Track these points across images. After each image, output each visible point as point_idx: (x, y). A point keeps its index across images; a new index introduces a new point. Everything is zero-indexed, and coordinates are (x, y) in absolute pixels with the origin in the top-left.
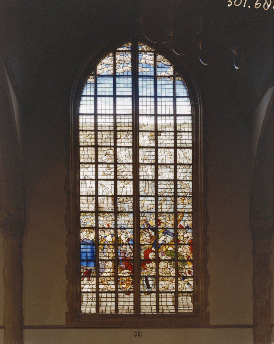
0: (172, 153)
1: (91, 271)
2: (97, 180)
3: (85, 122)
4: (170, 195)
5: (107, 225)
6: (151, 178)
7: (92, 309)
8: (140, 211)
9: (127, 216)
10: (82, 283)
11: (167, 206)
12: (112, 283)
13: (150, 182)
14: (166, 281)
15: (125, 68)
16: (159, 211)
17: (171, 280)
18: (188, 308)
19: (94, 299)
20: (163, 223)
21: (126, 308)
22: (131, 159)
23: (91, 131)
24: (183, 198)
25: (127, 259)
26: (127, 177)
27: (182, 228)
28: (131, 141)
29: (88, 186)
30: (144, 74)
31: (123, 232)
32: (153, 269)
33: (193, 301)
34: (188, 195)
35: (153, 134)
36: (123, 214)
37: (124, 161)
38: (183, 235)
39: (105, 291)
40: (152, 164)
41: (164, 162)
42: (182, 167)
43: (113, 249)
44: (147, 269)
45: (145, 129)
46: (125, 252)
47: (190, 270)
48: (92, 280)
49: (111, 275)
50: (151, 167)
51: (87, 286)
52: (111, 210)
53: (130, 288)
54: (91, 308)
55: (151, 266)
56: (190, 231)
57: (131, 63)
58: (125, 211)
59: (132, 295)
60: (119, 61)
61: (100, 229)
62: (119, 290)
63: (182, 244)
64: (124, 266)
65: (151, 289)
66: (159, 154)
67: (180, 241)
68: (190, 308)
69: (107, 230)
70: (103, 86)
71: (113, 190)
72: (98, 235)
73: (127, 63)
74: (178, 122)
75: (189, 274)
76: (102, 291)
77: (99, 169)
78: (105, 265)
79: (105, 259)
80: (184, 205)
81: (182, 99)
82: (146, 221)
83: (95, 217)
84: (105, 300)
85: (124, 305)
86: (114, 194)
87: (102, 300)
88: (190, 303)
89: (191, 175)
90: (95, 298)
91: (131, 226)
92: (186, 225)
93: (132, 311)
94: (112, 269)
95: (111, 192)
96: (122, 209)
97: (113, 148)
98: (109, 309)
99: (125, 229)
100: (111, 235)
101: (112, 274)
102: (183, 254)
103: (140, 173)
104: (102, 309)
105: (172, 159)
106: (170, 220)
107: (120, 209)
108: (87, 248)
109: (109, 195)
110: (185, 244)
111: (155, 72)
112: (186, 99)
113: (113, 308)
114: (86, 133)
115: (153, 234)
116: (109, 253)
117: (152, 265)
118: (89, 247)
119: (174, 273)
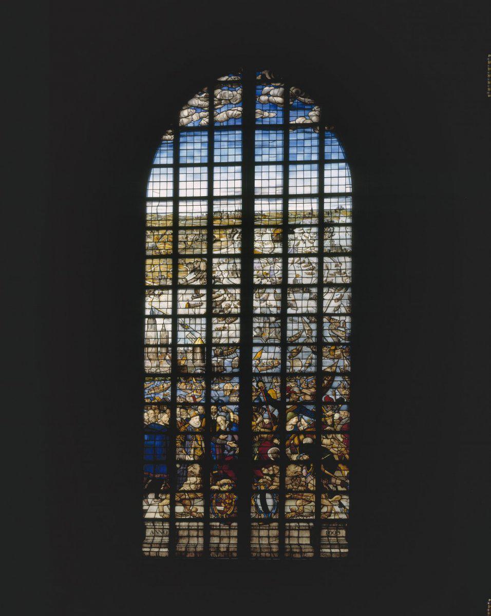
0: (314, 265)
1: (160, 481)
2: (175, 317)
3: (156, 212)
4: (308, 341)
5: (191, 398)
6: (274, 311)
7: (161, 550)
10: (144, 503)
11: (304, 361)
12: (198, 504)
13: (273, 319)
14: (298, 499)
15: (230, 112)
16: (288, 371)
17: (309, 498)
18: (337, 550)
19: (165, 532)
20: (295, 393)
21: (223, 548)
22: (238, 277)
23: (167, 228)
24: (333, 348)
25: (226, 459)
26: (229, 309)
27: (330, 402)
28: (238, 244)
30: (266, 121)
33: (347, 537)
34: (343, 341)
35: (279, 231)
37: (225, 282)
38: (333, 416)
39: (187, 517)
40: (274, 286)
41: (299, 281)
42: (333, 291)
45: (265, 222)
46: (223, 446)
47: (343, 479)
49: (198, 489)
50: (275, 291)
51: (154, 508)
52: (199, 371)
53: (233, 512)
54: (160, 548)
55: (271, 473)
56: (345, 407)
57: (241, 104)
58: (225, 372)
59: (235, 524)
60: (220, 100)
62: (213, 516)
63: (330, 432)
64: (221, 471)
66: (290, 267)
67: (326, 424)
68: (342, 550)
70: (190, 147)
71: (204, 334)
72: (176, 417)
73: (235, 104)
74: (327, 207)
75: (342, 487)
76: (180, 517)
77: (180, 297)
78: (187, 470)
79: (187, 459)
80: (336, 360)
81: (335, 166)
82: (265, 392)
84: (186, 533)
85: (220, 543)
87: (181, 533)
88: (343, 541)
89: (348, 305)
91: (234, 399)
92: (338, 397)
93: (235, 555)
95: (201, 338)
97: (206, 259)
98: (192, 549)
100: (198, 417)
101: (199, 486)
102: (332, 450)
103: (254, 302)
104: (180, 550)
105: (314, 276)
106: (308, 388)
107: (216, 368)
109: (197, 343)
110: (336, 432)
111: (286, 117)
112: (343, 165)
113: (200, 548)
114: (157, 233)
115: (276, 413)
117: (273, 470)
119: (315, 485)
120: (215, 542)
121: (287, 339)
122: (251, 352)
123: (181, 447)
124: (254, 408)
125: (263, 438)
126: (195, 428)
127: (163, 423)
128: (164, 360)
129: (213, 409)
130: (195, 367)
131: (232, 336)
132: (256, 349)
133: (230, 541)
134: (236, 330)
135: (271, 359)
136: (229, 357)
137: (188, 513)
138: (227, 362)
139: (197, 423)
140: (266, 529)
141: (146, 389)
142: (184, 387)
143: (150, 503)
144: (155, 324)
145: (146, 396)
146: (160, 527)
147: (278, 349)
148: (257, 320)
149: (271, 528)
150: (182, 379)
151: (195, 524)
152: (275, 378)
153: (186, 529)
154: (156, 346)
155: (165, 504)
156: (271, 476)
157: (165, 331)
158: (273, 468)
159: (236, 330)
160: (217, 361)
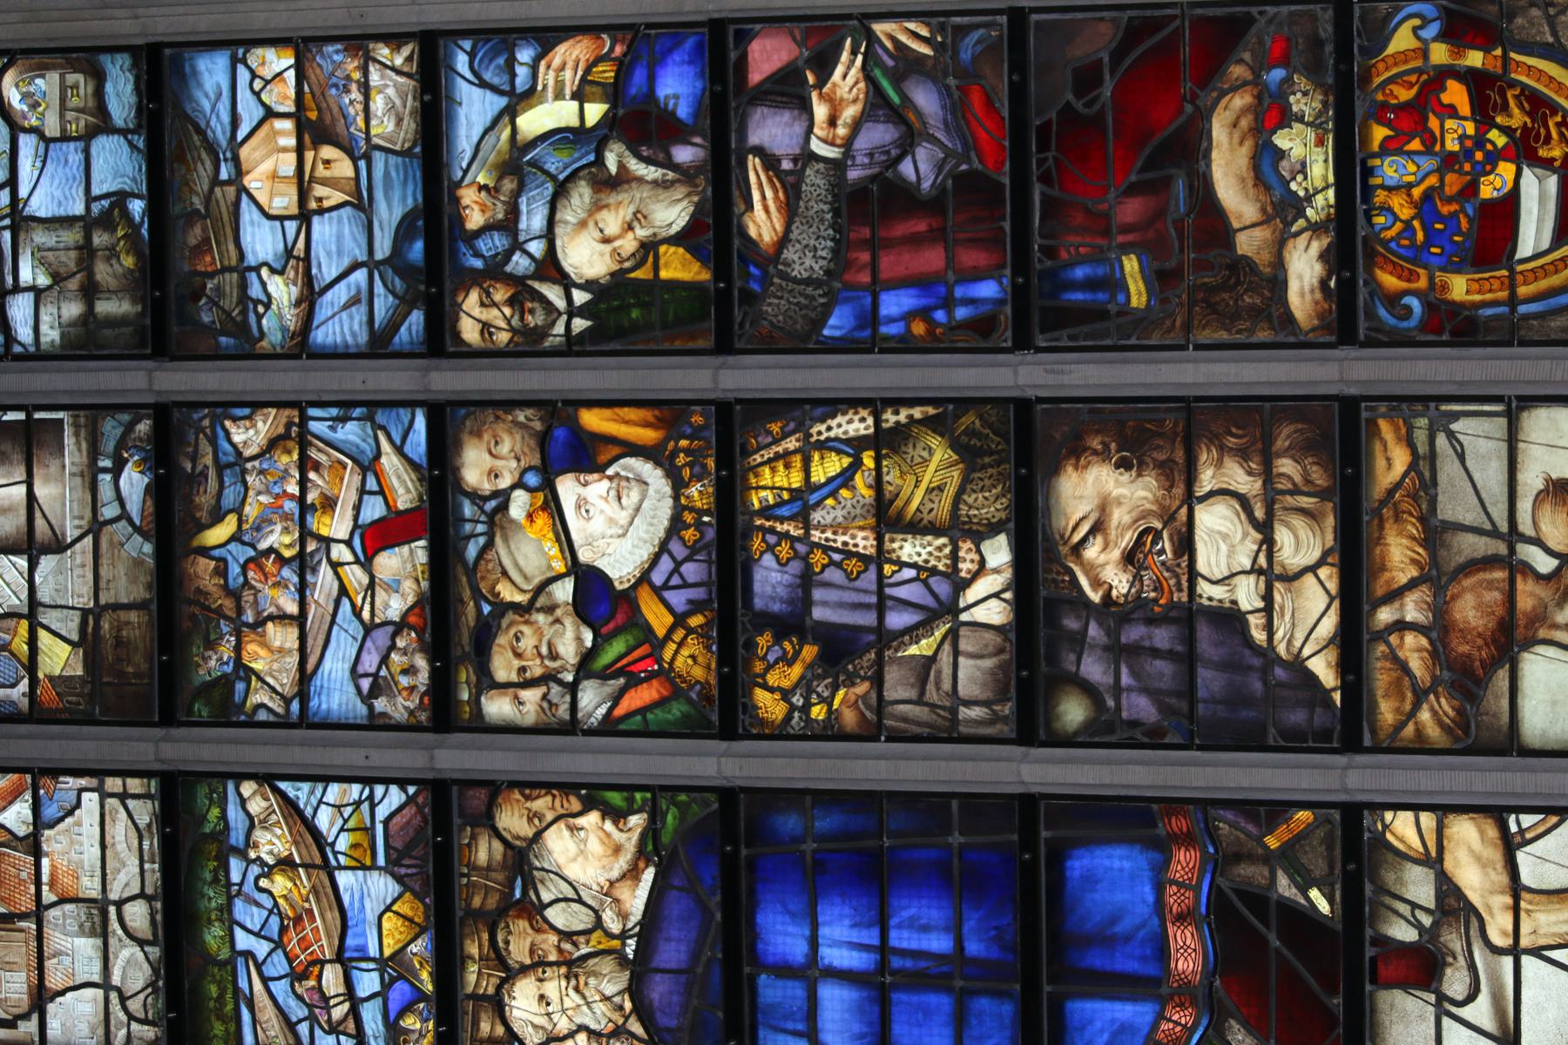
5: (389, 562)
9: (224, 175)
12: (1491, 476)
31: (498, 242)
36: (195, 235)
43: (819, 430)
48: (1419, 887)
49: (1319, 478)
52: (134, 482)
58: (137, 207)
61: (465, 696)
69: (472, 551)
79: (995, 613)
83: (248, 788)
100: (568, 488)
101: (1286, 466)
107: (104, 307)
108: (811, 973)
123: (878, 681)
127: (633, 874)
128: (37, 853)
129: (486, 328)
130: (96, 527)
155: (1503, 879)
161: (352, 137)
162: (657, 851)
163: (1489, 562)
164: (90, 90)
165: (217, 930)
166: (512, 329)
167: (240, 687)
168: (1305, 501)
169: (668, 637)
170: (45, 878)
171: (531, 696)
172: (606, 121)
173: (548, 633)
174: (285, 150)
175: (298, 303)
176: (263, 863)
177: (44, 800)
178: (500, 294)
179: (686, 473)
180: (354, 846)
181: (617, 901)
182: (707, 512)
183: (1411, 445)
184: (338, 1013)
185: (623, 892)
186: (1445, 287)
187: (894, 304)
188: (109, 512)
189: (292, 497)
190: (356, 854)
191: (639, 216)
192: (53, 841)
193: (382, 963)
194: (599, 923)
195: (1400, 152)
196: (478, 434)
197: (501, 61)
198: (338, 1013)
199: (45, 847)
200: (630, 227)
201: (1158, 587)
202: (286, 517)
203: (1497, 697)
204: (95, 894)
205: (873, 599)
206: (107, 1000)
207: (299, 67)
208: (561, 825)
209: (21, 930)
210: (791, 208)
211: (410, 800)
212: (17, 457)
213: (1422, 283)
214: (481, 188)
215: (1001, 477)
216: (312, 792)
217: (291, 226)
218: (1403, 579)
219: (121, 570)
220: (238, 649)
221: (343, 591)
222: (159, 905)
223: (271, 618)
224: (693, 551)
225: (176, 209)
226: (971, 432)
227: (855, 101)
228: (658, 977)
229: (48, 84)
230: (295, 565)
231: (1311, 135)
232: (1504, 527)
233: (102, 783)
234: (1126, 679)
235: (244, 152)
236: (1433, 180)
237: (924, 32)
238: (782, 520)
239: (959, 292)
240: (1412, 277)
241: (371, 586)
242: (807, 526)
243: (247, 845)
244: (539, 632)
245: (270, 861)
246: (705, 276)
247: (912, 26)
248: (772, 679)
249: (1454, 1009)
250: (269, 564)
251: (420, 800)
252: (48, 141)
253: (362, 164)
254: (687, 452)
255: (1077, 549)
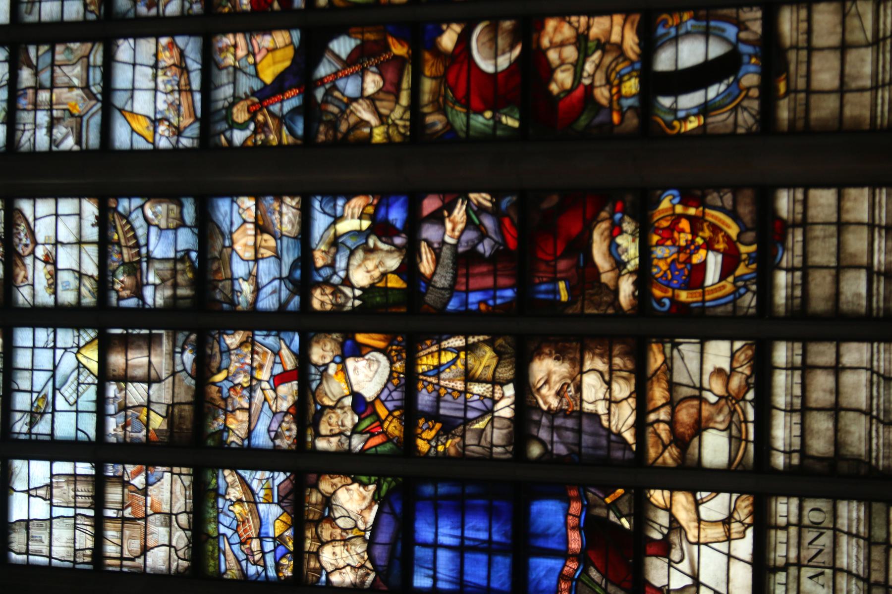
5: (283, 389)
8: (196, 143)
12: (693, 366)
13: (26, 76)
19: (816, 517)
25: (512, 244)
29: (40, 509)
32: (595, 32)
36: (215, 266)
39: (751, 416)
43: (445, 344)
44: (591, 88)
48: (663, 518)
49: (630, 365)
52: (189, 357)
53: (733, 214)
55: (570, 53)
58: (194, 255)
59: (784, 203)
61: (309, 439)
62: (749, 300)
64: (562, 265)
65: (746, 42)
69: (314, 385)
71: (66, 337)
72: (349, 452)
76: (751, 447)
78: (552, 414)
79: (508, 413)
83: (227, 472)
84: (822, 424)
85: (869, 268)
86: (93, 333)
87: (820, 445)
90: (809, 504)
94: (587, 356)
95: (79, 348)
96: (180, 279)
99: (305, 259)
100: (350, 363)
101: (617, 361)
107: (181, 292)
108: (435, 546)
109: (94, 366)
115: (343, 46)
116: (469, 377)
117: (562, 44)
118: (425, 532)
120: (863, 290)
121: (91, 17)
122: (132, 153)
123: (463, 437)
124: (322, 137)
125: (436, 93)
126: (391, 372)
127: (369, 507)
129: (322, 303)
130: (174, 374)
131: (75, 231)
132: (122, 137)
133: (860, 224)
134: (57, 215)
135: (155, 77)
136: (142, 241)
137: (732, 412)
138: (160, 247)
139: (374, 367)
140: (809, 63)
141: (243, 572)
142: (242, 416)
143: (688, 581)
144: (27, 523)
145: (272, 573)
146: (794, 541)
147: (124, 50)
148: (28, 134)
149: (803, 38)
150: (218, 425)
151: (780, 379)
152: (219, 57)
153: (803, 424)
154: (99, 523)
155: (694, 516)
156: (584, 54)
157: (50, 486)
158: (553, 45)
159: (57, 215)
160: (156, 286)
161: (275, 232)
162: (379, 499)
163: (692, 398)
164: (178, 211)
165: (213, 526)
166: (332, 304)
167: (225, 434)
168: (624, 374)
169: (386, 419)
170: (149, 504)
171: (334, 440)
172: (369, 228)
173: (342, 416)
174: (250, 235)
175: (253, 292)
176: (231, 501)
177: (150, 476)
178: (328, 290)
179: (395, 358)
180: (266, 495)
181: (363, 517)
182: (402, 373)
183: (664, 353)
184: (257, 557)
185: (366, 514)
186: (678, 296)
187: (474, 298)
188: (179, 368)
189: (248, 364)
190: (266, 498)
191: (381, 263)
192: (152, 490)
193: (274, 539)
194: (356, 526)
195: (663, 245)
196: (318, 342)
197: (332, 204)
198: (257, 557)
199: (149, 493)
200: (377, 267)
201: (568, 404)
202: (245, 371)
203: (694, 448)
204: (167, 511)
205: (463, 407)
206: (170, 551)
207: (257, 205)
208: (344, 489)
209: (139, 524)
210: (437, 261)
211: (288, 478)
212: (145, 347)
213: (670, 294)
214: (323, 251)
215: (510, 363)
216: (251, 474)
217: (251, 264)
218: (660, 403)
219: (183, 390)
220: (225, 420)
221: (265, 400)
222: (191, 516)
223: (238, 409)
224: (397, 387)
225: (209, 256)
226: (501, 346)
227: (462, 222)
228: (378, 546)
229: (161, 208)
230: (248, 389)
231: (630, 238)
232: (698, 385)
233: (172, 469)
234: (555, 438)
235: (235, 236)
236: (675, 256)
237: (488, 197)
238: (430, 376)
239: (498, 293)
240: (666, 292)
241: (276, 398)
242: (439, 379)
243: (226, 494)
244: (338, 416)
245: (234, 500)
246: (404, 286)
247: (484, 195)
248: (424, 435)
249: (675, 565)
250: (238, 388)
251: (292, 478)
252: (161, 229)
253: (279, 241)
254: (396, 351)
255: (539, 390)
